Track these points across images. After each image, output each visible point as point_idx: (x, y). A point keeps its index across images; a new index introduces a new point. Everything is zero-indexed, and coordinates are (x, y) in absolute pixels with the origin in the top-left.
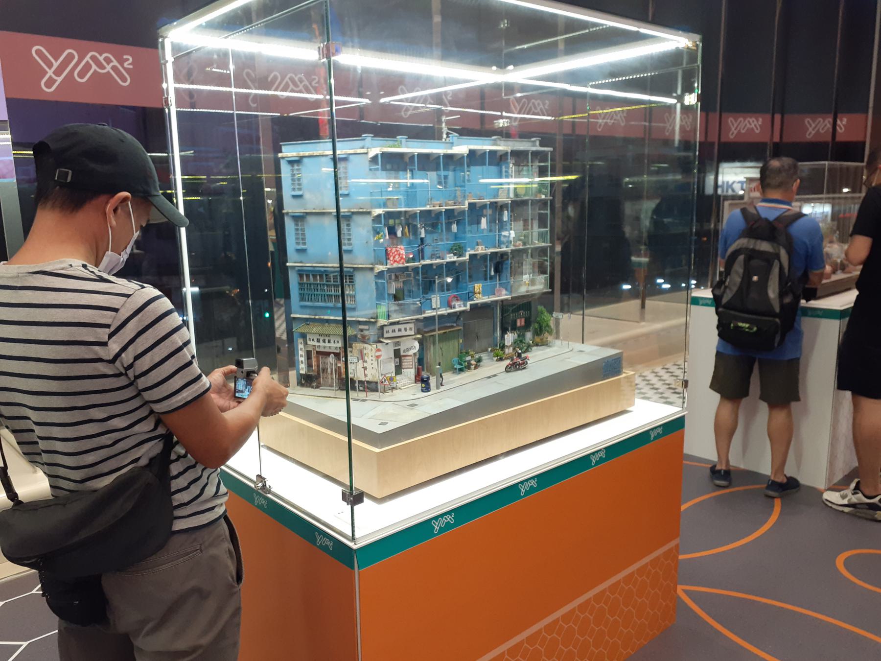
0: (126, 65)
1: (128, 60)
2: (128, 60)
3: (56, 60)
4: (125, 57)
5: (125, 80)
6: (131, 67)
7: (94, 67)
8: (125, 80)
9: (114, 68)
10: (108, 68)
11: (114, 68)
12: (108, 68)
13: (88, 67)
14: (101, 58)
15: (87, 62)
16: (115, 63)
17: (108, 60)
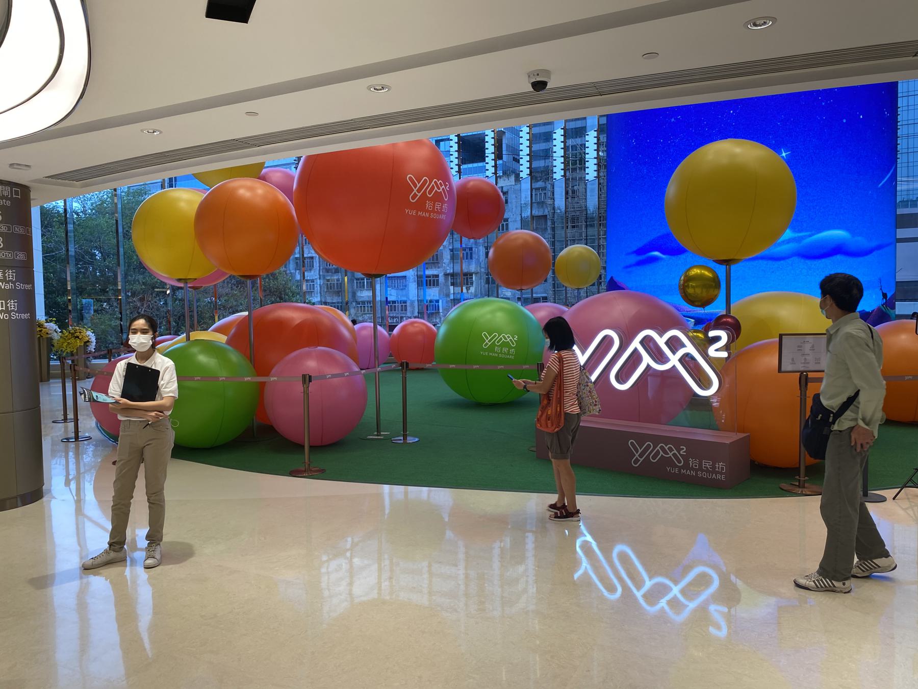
0: (712, 351)
1: (718, 339)
2: (718, 339)
3: (583, 353)
4: (712, 334)
5: (704, 382)
6: (724, 354)
7: (647, 360)
8: (704, 382)
9: (687, 360)
10: (674, 360)
11: (687, 360)
12: (674, 360)
13: (635, 359)
14: (661, 341)
15: (636, 350)
16: (690, 349)
17: (674, 344)
